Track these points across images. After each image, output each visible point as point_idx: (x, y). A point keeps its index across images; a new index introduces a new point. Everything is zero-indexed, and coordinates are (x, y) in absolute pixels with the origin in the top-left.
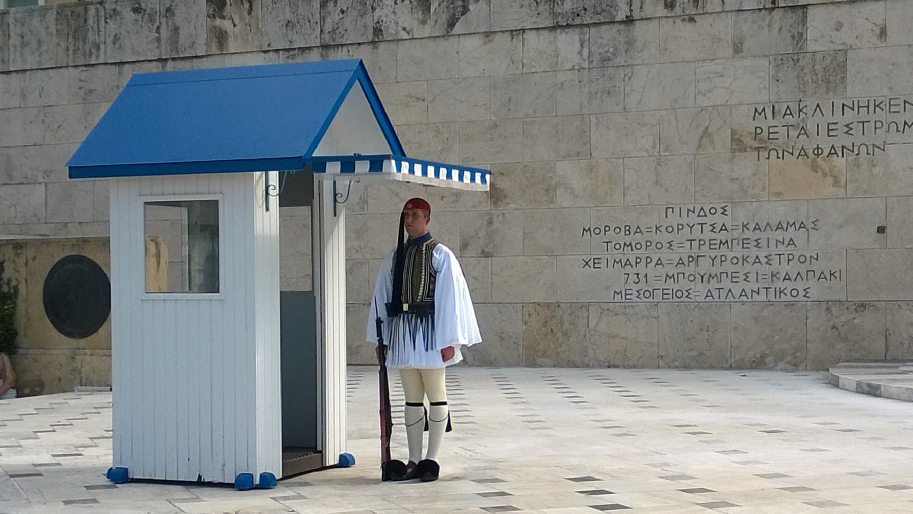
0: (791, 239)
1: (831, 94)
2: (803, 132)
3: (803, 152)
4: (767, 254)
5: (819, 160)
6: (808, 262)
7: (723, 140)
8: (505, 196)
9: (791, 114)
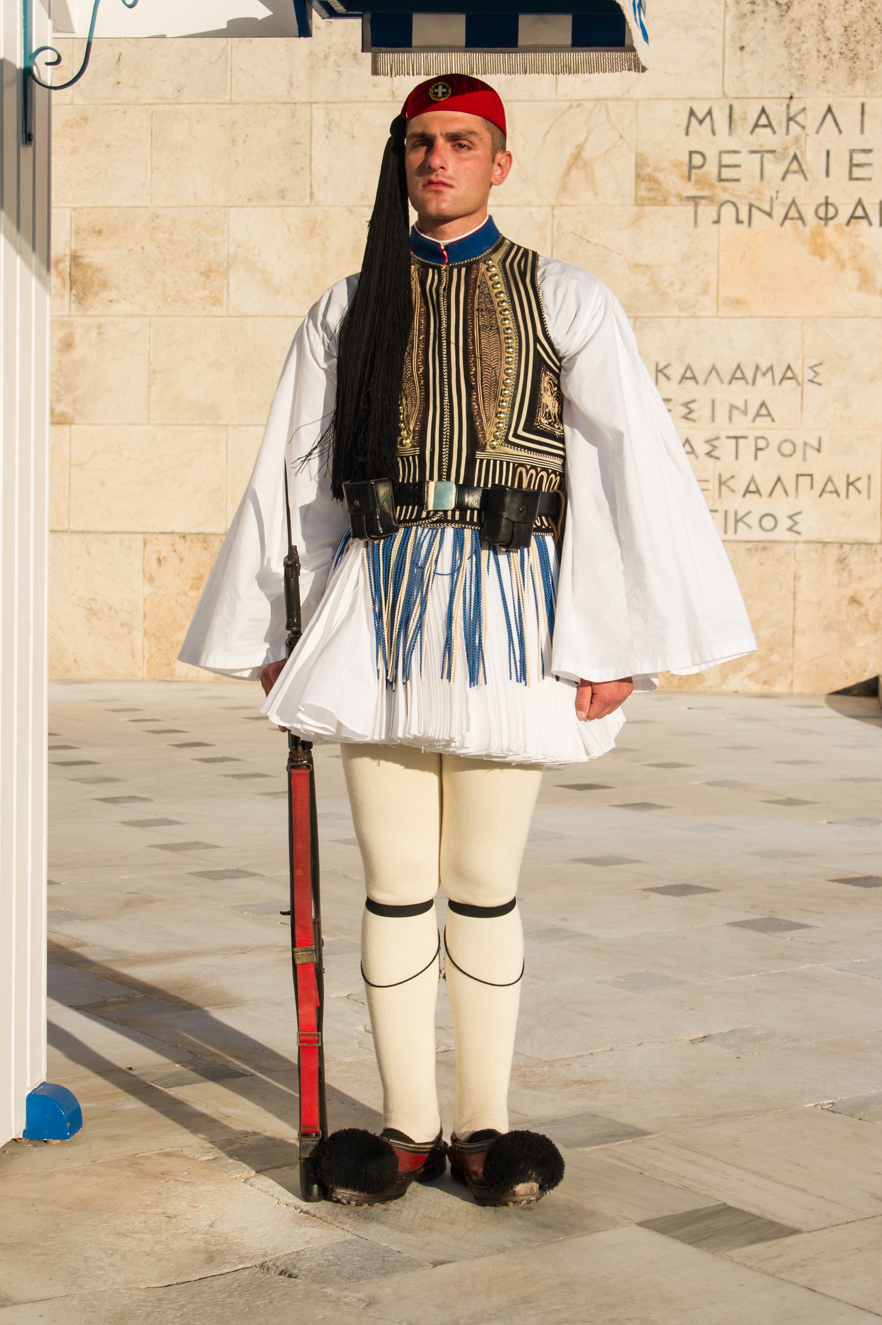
0: (763, 404)
1: (859, 85)
2: (795, 167)
3: (793, 213)
4: (709, 435)
5: (830, 231)
6: (799, 453)
7: (616, 178)
8: (105, 285)
9: (770, 125)
